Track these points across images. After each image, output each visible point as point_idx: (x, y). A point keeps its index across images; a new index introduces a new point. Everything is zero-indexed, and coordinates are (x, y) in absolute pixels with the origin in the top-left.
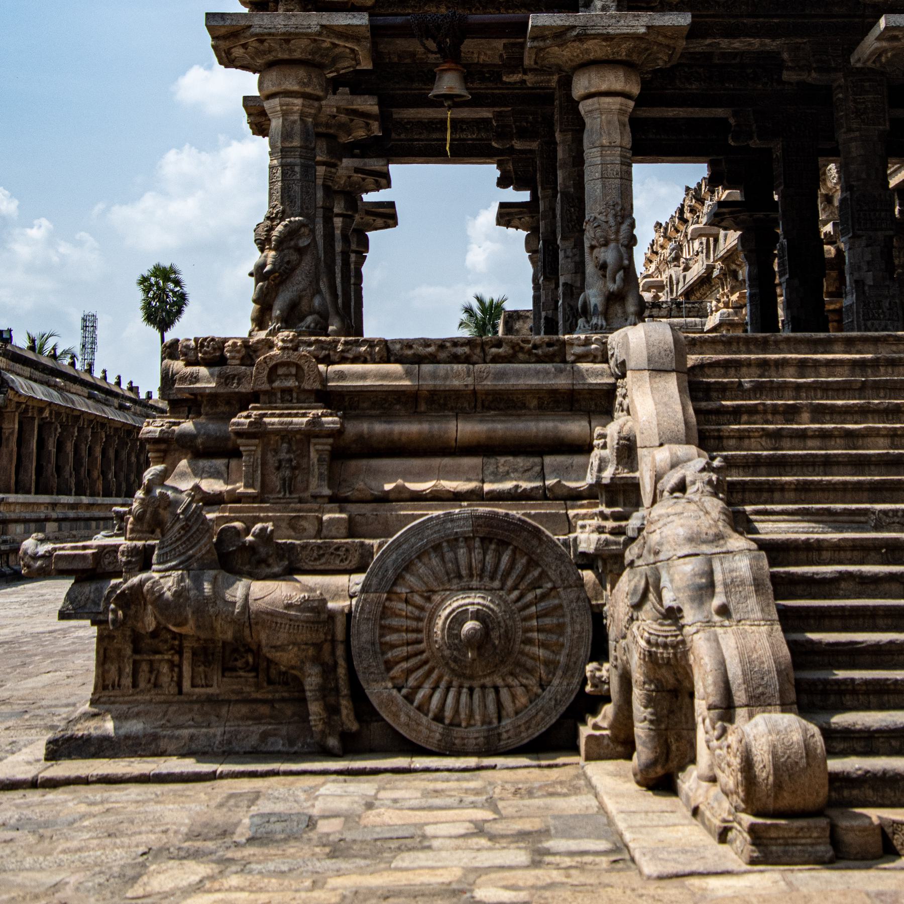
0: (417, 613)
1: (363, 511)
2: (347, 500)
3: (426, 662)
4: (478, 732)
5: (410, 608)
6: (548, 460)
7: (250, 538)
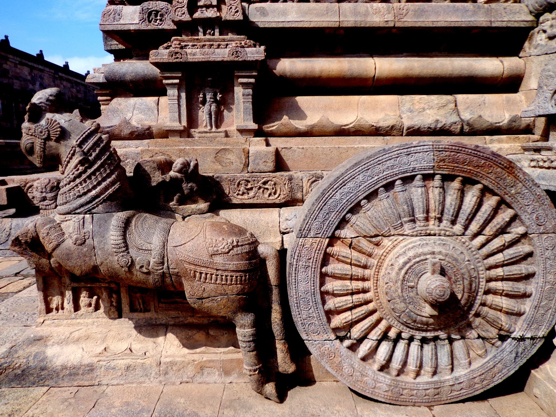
1: (288, 146)
4: (428, 383)
5: (355, 254)
6: (461, 98)
7: (172, 173)
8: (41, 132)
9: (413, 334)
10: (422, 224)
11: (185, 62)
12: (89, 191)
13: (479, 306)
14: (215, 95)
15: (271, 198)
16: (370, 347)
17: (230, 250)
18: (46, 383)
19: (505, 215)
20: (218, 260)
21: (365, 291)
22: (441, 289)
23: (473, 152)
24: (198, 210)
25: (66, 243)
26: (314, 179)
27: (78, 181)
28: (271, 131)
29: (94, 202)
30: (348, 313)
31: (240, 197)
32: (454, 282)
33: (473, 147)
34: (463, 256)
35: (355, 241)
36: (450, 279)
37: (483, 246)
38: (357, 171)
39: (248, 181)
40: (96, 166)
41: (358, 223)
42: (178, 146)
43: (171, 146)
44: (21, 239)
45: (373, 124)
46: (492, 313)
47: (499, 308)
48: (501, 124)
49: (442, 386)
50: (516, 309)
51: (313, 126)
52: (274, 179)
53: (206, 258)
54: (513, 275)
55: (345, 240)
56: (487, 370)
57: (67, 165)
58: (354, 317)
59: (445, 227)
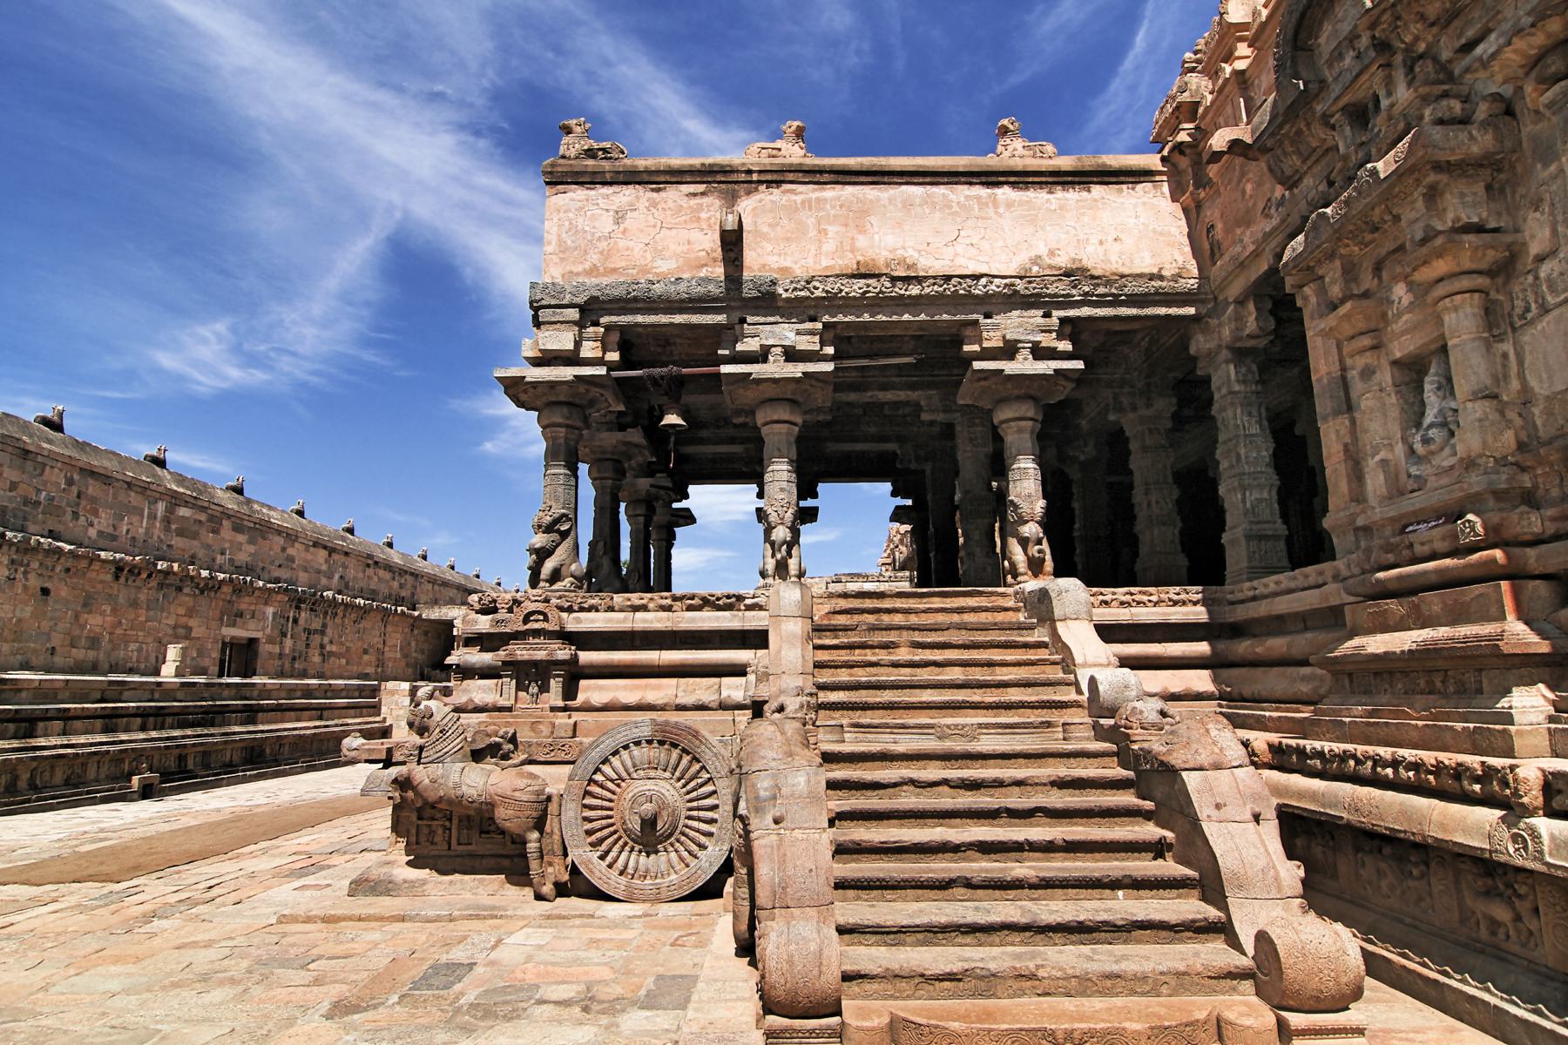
0: (609, 795)
5: (605, 793)
6: (725, 680)
19: (697, 766)
20: (517, 794)
46: (692, 833)
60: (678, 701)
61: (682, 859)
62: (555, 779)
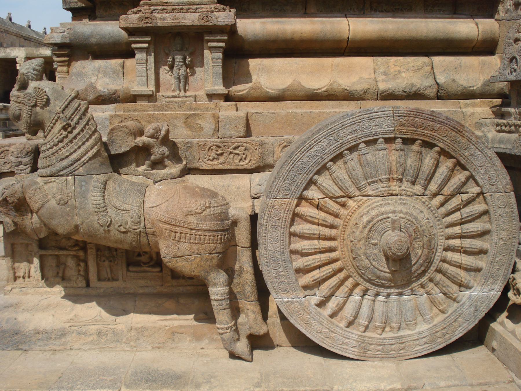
0: (330, 219)
1: (259, 111)
2: (242, 99)
3: (340, 270)
5: (322, 215)
6: (437, 59)
8: (29, 100)
9: (379, 290)
10: (385, 185)
11: (155, 27)
12: (71, 154)
13: (439, 262)
14: (184, 59)
15: (241, 163)
16: (338, 304)
17: (204, 210)
18: (20, 347)
19: (460, 177)
20: (192, 219)
21: (332, 250)
22: (399, 243)
23: (429, 117)
24: (170, 174)
25: (50, 202)
26: (285, 144)
27: (61, 145)
28: (241, 95)
29: (75, 165)
30: (317, 271)
31: (210, 162)
32: (414, 239)
33: (429, 113)
34: (422, 215)
35: (322, 201)
36: (410, 236)
37: (442, 205)
38: (322, 135)
39: (219, 147)
40: (75, 132)
41: (324, 184)
42: (147, 111)
43: (140, 111)
44: (8, 199)
45: (346, 88)
47: (458, 264)
48: (475, 88)
49: (406, 340)
50: (473, 265)
51: (284, 91)
52: (244, 144)
53: (180, 218)
54: (470, 232)
55: (313, 201)
56: (448, 324)
57: (50, 131)
58: (322, 275)
59: (406, 187)
60: (382, 86)
61: (433, 302)
62: (240, 194)
